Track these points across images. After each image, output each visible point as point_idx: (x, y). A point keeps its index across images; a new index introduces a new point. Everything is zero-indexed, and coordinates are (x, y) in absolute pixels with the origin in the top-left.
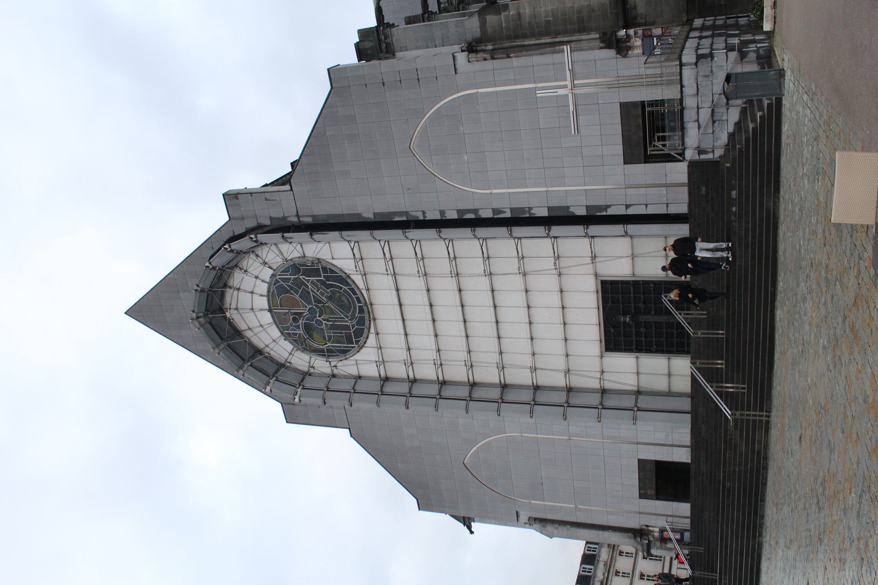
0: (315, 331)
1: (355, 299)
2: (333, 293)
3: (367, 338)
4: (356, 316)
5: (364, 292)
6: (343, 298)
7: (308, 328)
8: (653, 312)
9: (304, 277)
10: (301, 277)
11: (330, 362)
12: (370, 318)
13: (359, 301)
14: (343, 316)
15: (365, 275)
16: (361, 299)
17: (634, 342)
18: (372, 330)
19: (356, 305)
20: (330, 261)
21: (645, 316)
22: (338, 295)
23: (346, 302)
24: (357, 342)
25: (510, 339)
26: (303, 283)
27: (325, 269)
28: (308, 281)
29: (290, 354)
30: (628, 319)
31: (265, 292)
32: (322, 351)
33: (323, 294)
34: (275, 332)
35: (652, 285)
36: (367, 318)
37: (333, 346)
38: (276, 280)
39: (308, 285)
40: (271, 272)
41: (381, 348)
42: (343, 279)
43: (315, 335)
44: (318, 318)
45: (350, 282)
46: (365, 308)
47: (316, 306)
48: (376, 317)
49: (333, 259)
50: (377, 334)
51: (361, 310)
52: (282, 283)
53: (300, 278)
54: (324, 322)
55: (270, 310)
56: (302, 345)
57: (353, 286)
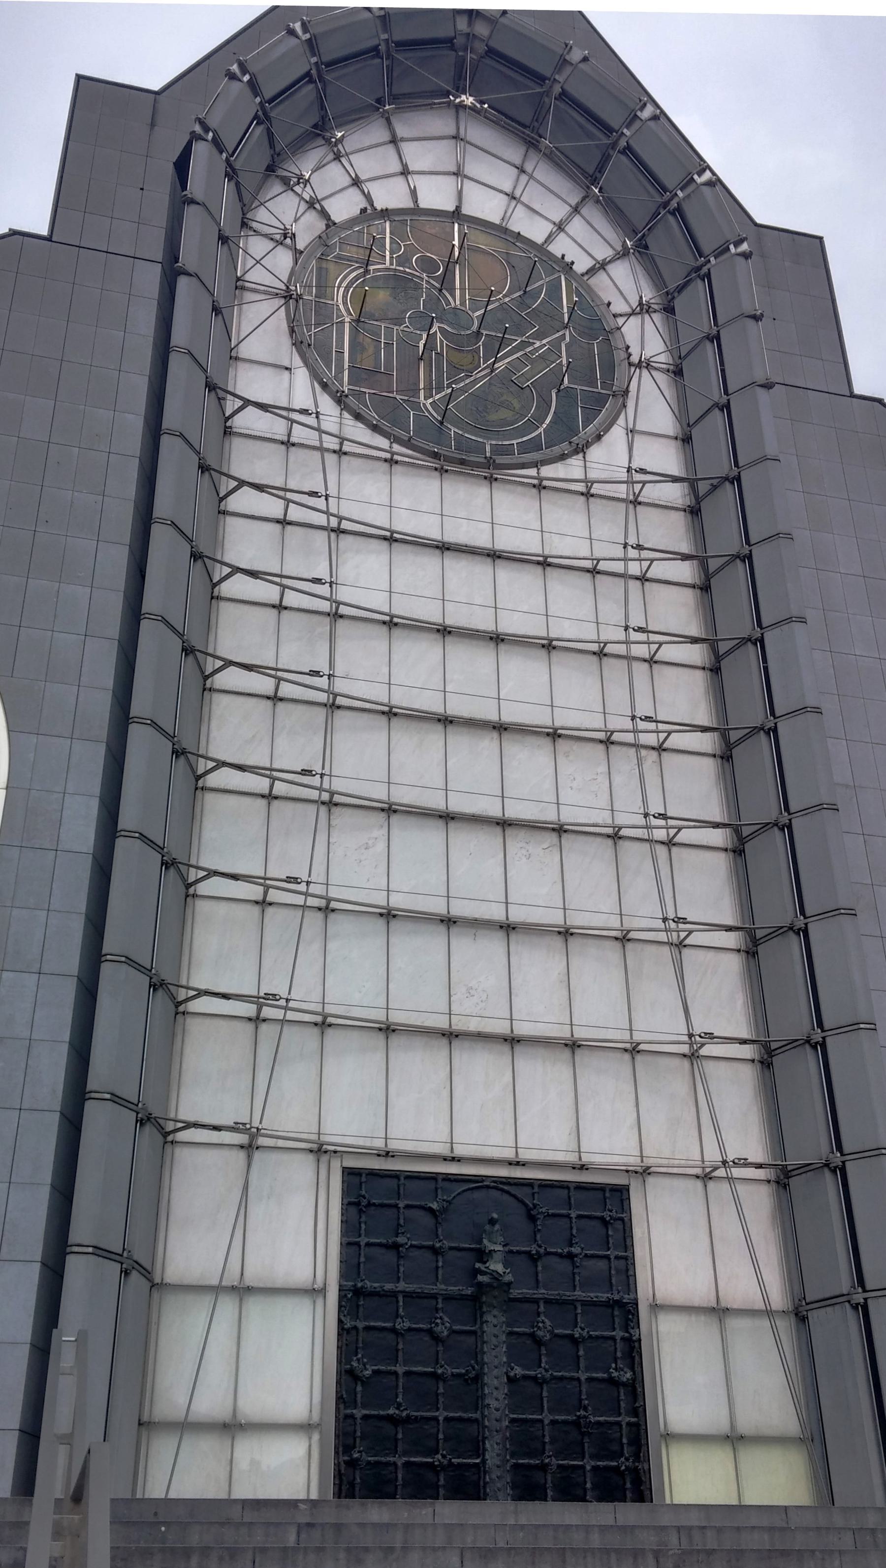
0: (391, 299)
1: (533, 435)
4: (449, 426)
8: (518, 1371)
9: (568, 339)
15: (588, 495)
17: (388, 1286)
19: (489, 439)
21: (503, 1337)
25: (381, 846)
30: (496, 1266)
35: (629, 1375)
39: (544, 342)
40: (582, 265)
45: (557, 450)
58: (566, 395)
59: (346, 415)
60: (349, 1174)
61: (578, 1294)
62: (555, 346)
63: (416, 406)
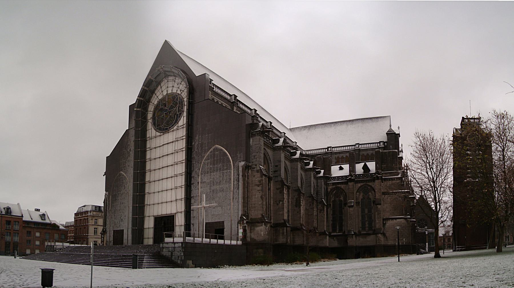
3: (159, 132)
5: (172, 130)
6: (171, 122)
7: (161, 110)
10: (178, 105)
11: (151, 119)
12: (164, 132)
13: (169, 128)
14: (165, 122)
16: (170, 128)
18: (161, 134)
20: (183, 116)
22: (172, 119)
23: (169, 123)
26: (176, 105)
27: (180, 114)
28: (177, 108)
29: (153, 104)
31: (173, 92)
34: (160, 97)
36: (164, 131)
41: (156, 137)
42: (177, 122)
43: (160, 112)
44: (164, 113)
45: (175, 124)
46: (167, 130)
48: (164, 135)
49: (183, 117)
50: (160, 136)
51: (167, 129)
52: (176, 98)
56: (157, 107)
57: (174, 125)
58: (177, 115)
59: (157, 132)
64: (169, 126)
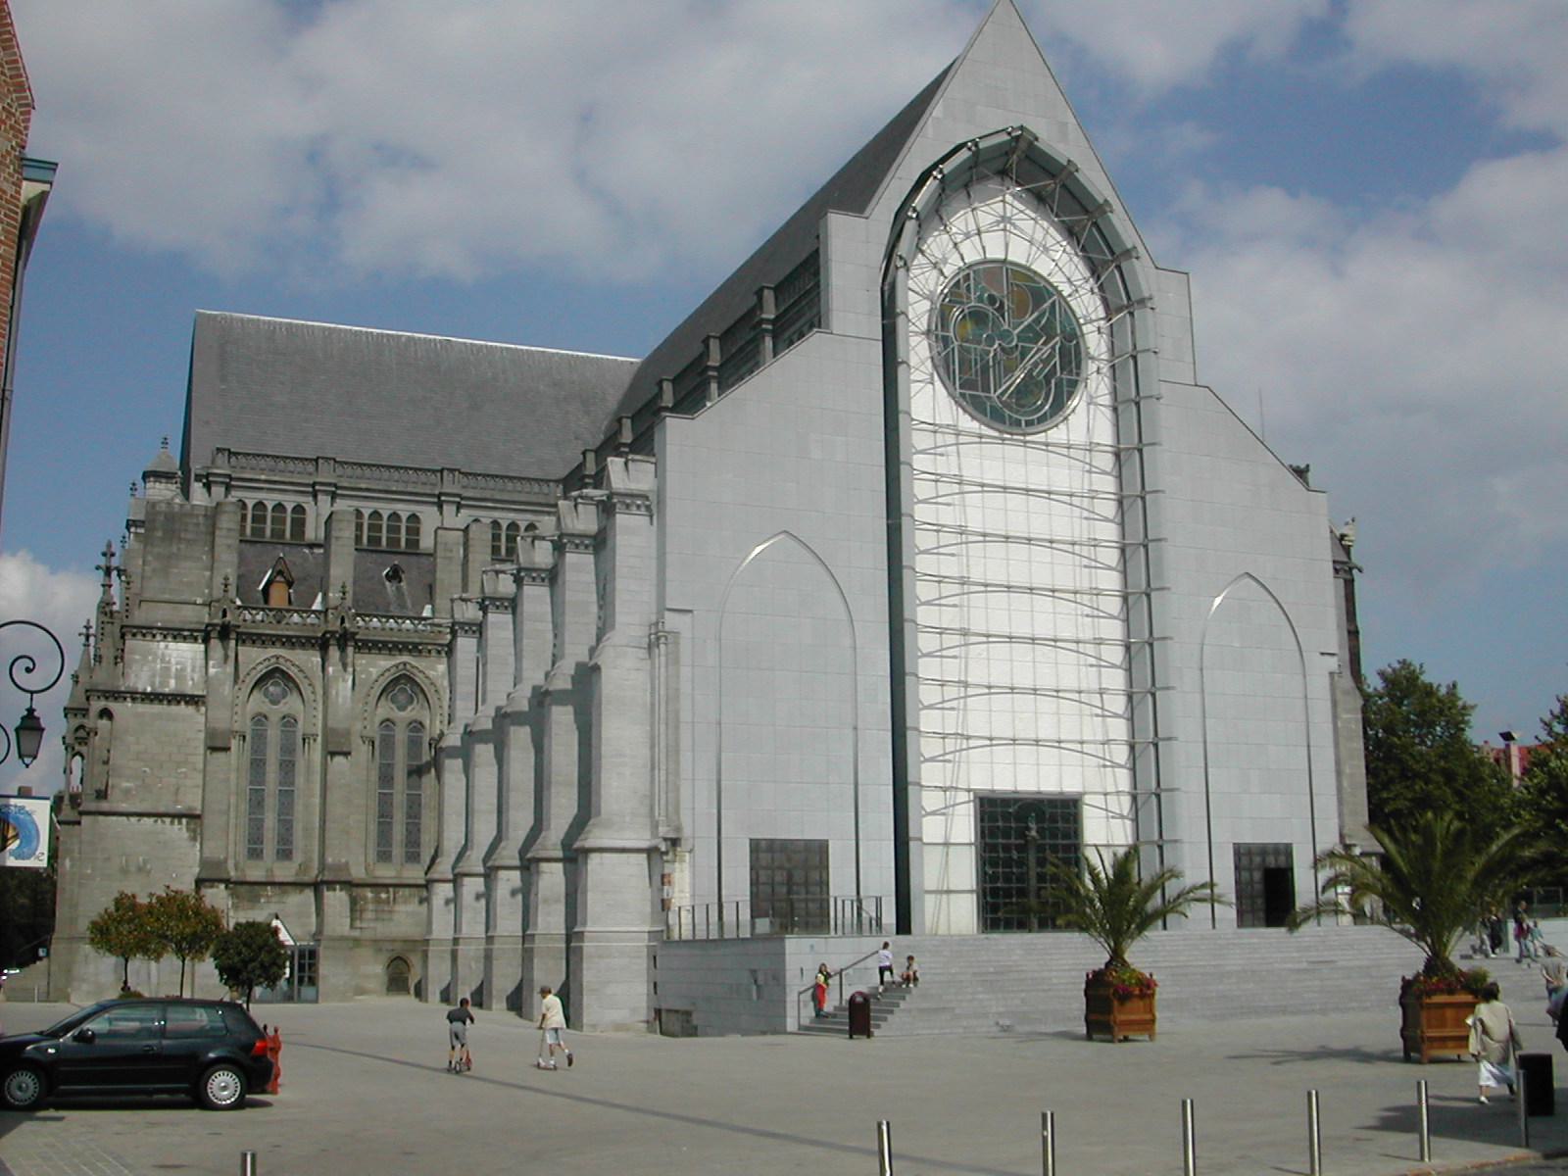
2: (1037, 384)
7: (978, 317)
10: (1057, 339)
13: (1029, 423)
18: (986, 430)
24: (963, 395)
28: (1053, 348)
32: (944, 326)
33: (1036, 364)
37: (953, 349)
38: (1051, 295)
40: (1065, 294)
44: (997, 342)
47: (1017, 346)
51: (1018, 423)
53: (1057, 335)
54: (992, 349)
55: (1005, 261)
60: (982, 799)
61: (1060, 841)
62: (1053, 348)
63: (989, 398)
64: (1025, 414)
